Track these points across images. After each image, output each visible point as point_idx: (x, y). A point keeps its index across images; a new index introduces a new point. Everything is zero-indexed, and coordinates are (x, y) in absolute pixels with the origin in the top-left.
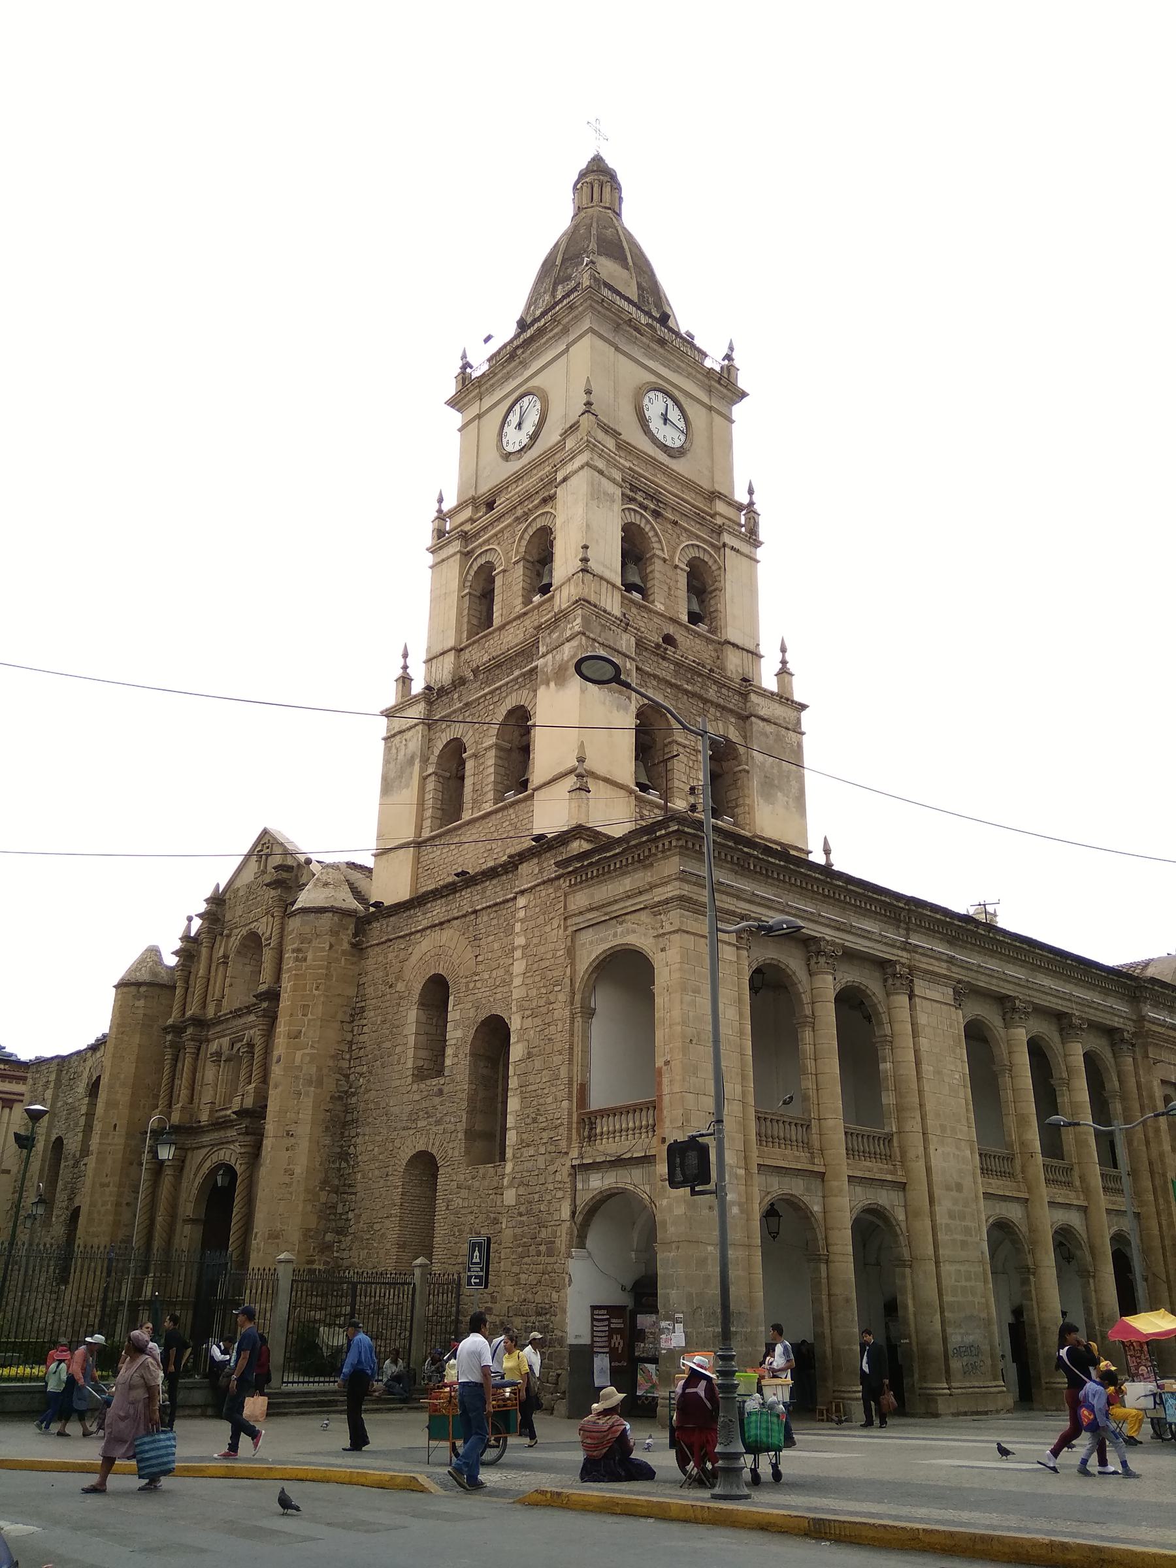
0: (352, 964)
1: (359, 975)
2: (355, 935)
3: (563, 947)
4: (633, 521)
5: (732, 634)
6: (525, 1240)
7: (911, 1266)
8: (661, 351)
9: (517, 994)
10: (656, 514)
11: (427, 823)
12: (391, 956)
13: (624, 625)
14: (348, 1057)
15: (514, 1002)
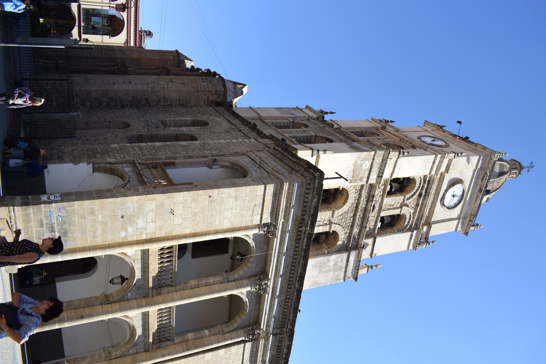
0: (204, 102)
1: (200, 106)
2: (216, 101)
3: (239, 151)
4: (417, 183)
5: (379, 240)
6: (95, 151)
7: (105, 360)
8: (477, 190)
9: (210, 142)
10: (420, 195)
11: (270, 121)
12: (211, 112)
13: (381, 175)
14: (165, 104)
15: (205, 141)
